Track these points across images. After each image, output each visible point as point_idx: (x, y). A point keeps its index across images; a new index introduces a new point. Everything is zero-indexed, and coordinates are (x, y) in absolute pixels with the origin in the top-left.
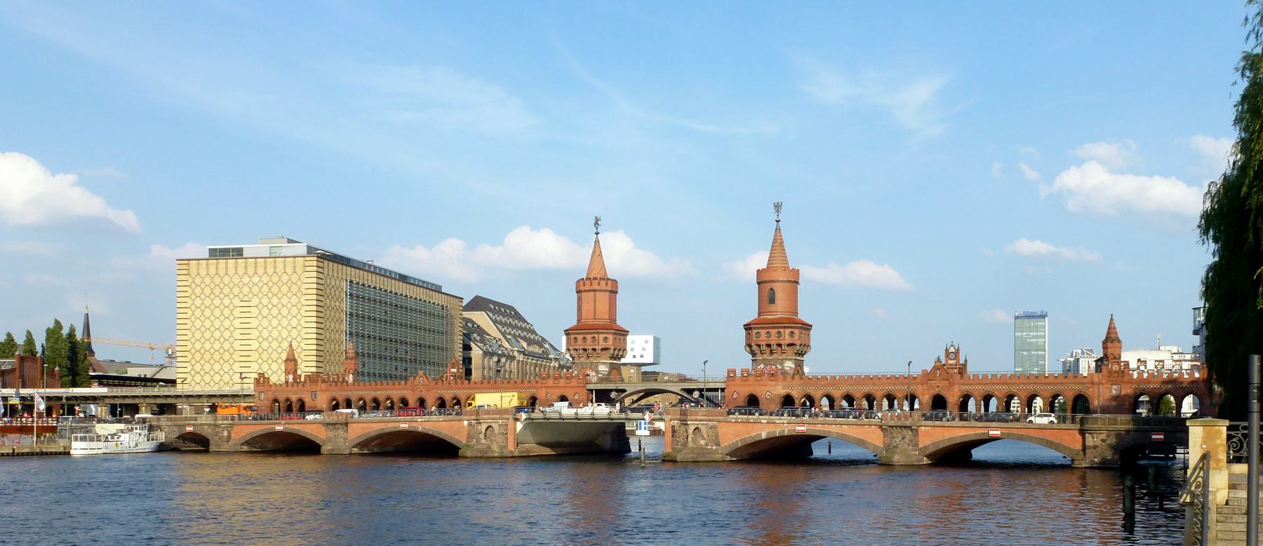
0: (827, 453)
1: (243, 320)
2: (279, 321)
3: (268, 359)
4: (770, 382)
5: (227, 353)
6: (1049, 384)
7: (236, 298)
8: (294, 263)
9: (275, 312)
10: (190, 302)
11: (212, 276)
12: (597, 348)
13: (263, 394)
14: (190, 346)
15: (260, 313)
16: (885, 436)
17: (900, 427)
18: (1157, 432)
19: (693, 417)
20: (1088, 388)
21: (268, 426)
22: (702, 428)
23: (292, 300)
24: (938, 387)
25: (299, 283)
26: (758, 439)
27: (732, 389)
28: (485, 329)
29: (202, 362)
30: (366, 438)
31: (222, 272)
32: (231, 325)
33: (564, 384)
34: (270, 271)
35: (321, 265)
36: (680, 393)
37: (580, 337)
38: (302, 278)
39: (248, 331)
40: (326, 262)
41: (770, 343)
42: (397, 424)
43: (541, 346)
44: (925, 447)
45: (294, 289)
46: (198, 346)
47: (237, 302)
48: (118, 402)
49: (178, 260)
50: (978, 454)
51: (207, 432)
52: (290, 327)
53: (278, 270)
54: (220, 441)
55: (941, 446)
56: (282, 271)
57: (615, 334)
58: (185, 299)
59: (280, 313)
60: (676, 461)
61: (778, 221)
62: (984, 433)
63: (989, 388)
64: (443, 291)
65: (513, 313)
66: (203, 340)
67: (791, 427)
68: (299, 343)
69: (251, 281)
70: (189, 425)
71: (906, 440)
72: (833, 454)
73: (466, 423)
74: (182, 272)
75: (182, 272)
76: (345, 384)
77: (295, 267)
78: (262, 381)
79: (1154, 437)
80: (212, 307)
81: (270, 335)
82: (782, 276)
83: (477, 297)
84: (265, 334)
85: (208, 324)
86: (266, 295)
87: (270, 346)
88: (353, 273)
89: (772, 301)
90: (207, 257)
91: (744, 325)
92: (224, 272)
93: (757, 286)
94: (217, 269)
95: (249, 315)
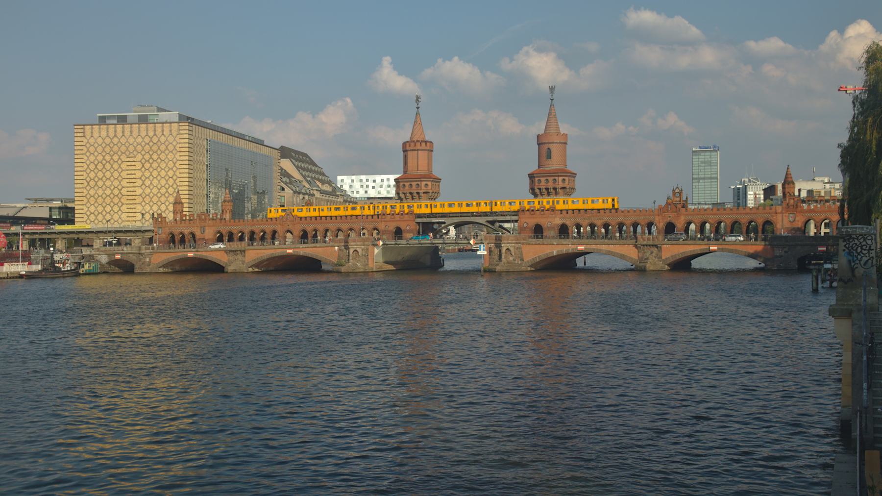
0: (583, 265)
1: (129, 172)
3: (149, 202)
4: (551, 216)
5: (116, 198)
6: (747, 214)
7: (124, 155)
8: (171, 127)
9: (155, 165)
10: (86, 158)
11: (104, 137)
12: (420, 192)
13: (160, 230)
14: (85, 192)
15: (143, 166)
16: (638, 252)
17: (650, 245)
18: (822, 246)
19: (505, 241)
20: (773, 216)
21: (181, 254)
22: (512, 249)
23: (169, 157)
24: (670, 217)
25: (175, 143)
26: (551, 256)
27: (523, 220)
28: (290, 173)
29: (96, 205)
30: (259, 260)
31: (112, 134)
32: (120, 175)
33: (398, 219)
34: (151, 133)
35: (191, 129)
36: (485, 224)
37: (407, 184)
38: (177, 139)
39: (133, 180)
40: (194, 126)
41: (548, 187)
42: (284, 250)
43: (331, 186)
44: (666, 259)
46: (92, 192)
47: (124, 158)
48: (37, 237)
50: (696, 264)
51: (132, 258)
53: (157, 133)
54: (142, 266)
55: (678, 257)
57: (432, 181)
58: (81, 156)
59: (159, 166)
60: (495, 272)
61: (552, 100)
62: (707, 249)
63: (705, 218)
64: (265, 144)
65: (308, 159)
66: (96, 188)
67: (574, 247)
69: (135, 141)
70: (118, 254)
71: (654, 254)
72: (587, 265)
73: (336, 248)
74: (78, 135)
75: (78, 135)
76: (223, 221)
77: (171, 130)
78: (158, 219)
79: (820, 249)
80: (104, 162)
81: (151, 183)
82: (556, 139)
83: (282, 146)
84: (147, 182)
85: (100, 175)
86: (148, 152)
87: (151, 192)
88: (211, 134)
89: (549, 156)
90: (98, 122)
91: (529, 175)
93: (537, 146)
94: (108, 132)
95: (134, 168)
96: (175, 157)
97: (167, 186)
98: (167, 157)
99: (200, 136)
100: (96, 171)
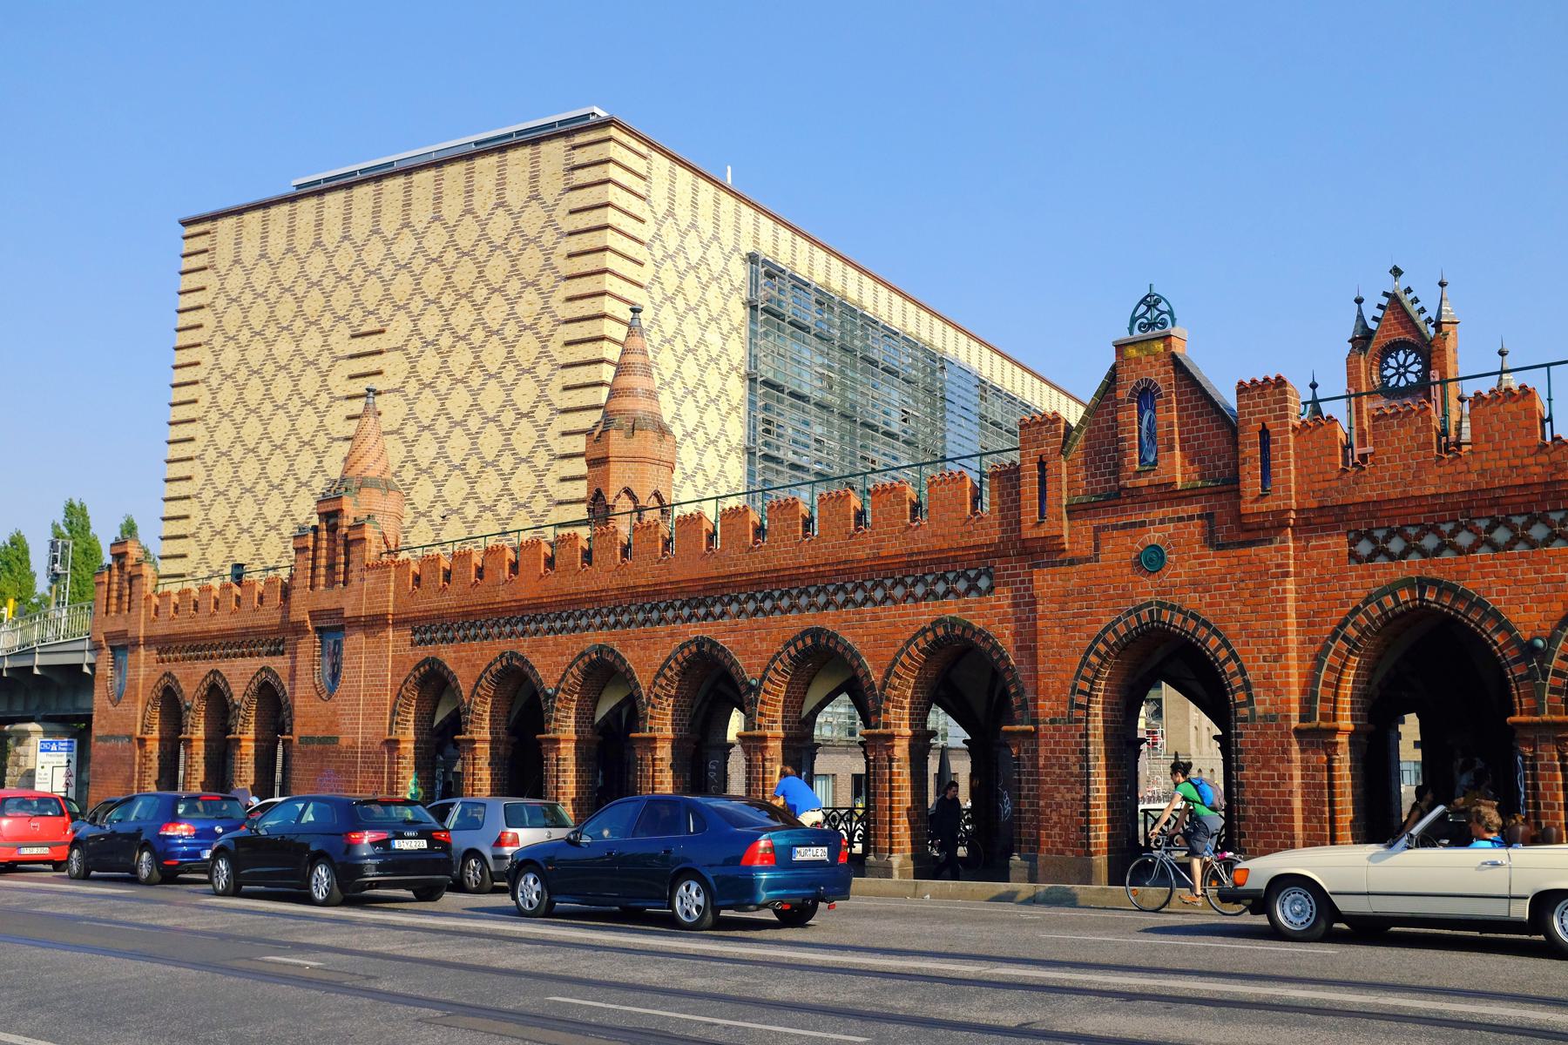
2: (475, 394)
7: (342, 325)
11: (275, 258)
15: (413, 371)
23: (521, 309)
40: (660, 163)
45: (531, 262)
47: (342, 343)
49: (186, 223)
52: (512, 415)
53: (478, 201)
56: (490, 205)
59: (477, 363)
68: (540, 476)
74: (194, 262)
77: (534, 178)
92: (311, 241)
96: (546, 308)
97: (506, 463)
98: (512, 314)
99: (706, 226)
100: (240, 412)
